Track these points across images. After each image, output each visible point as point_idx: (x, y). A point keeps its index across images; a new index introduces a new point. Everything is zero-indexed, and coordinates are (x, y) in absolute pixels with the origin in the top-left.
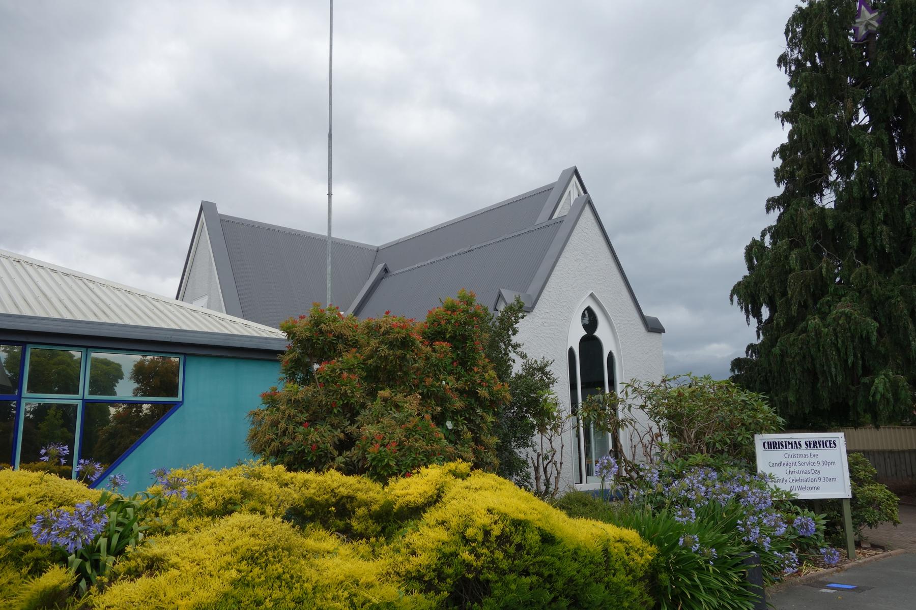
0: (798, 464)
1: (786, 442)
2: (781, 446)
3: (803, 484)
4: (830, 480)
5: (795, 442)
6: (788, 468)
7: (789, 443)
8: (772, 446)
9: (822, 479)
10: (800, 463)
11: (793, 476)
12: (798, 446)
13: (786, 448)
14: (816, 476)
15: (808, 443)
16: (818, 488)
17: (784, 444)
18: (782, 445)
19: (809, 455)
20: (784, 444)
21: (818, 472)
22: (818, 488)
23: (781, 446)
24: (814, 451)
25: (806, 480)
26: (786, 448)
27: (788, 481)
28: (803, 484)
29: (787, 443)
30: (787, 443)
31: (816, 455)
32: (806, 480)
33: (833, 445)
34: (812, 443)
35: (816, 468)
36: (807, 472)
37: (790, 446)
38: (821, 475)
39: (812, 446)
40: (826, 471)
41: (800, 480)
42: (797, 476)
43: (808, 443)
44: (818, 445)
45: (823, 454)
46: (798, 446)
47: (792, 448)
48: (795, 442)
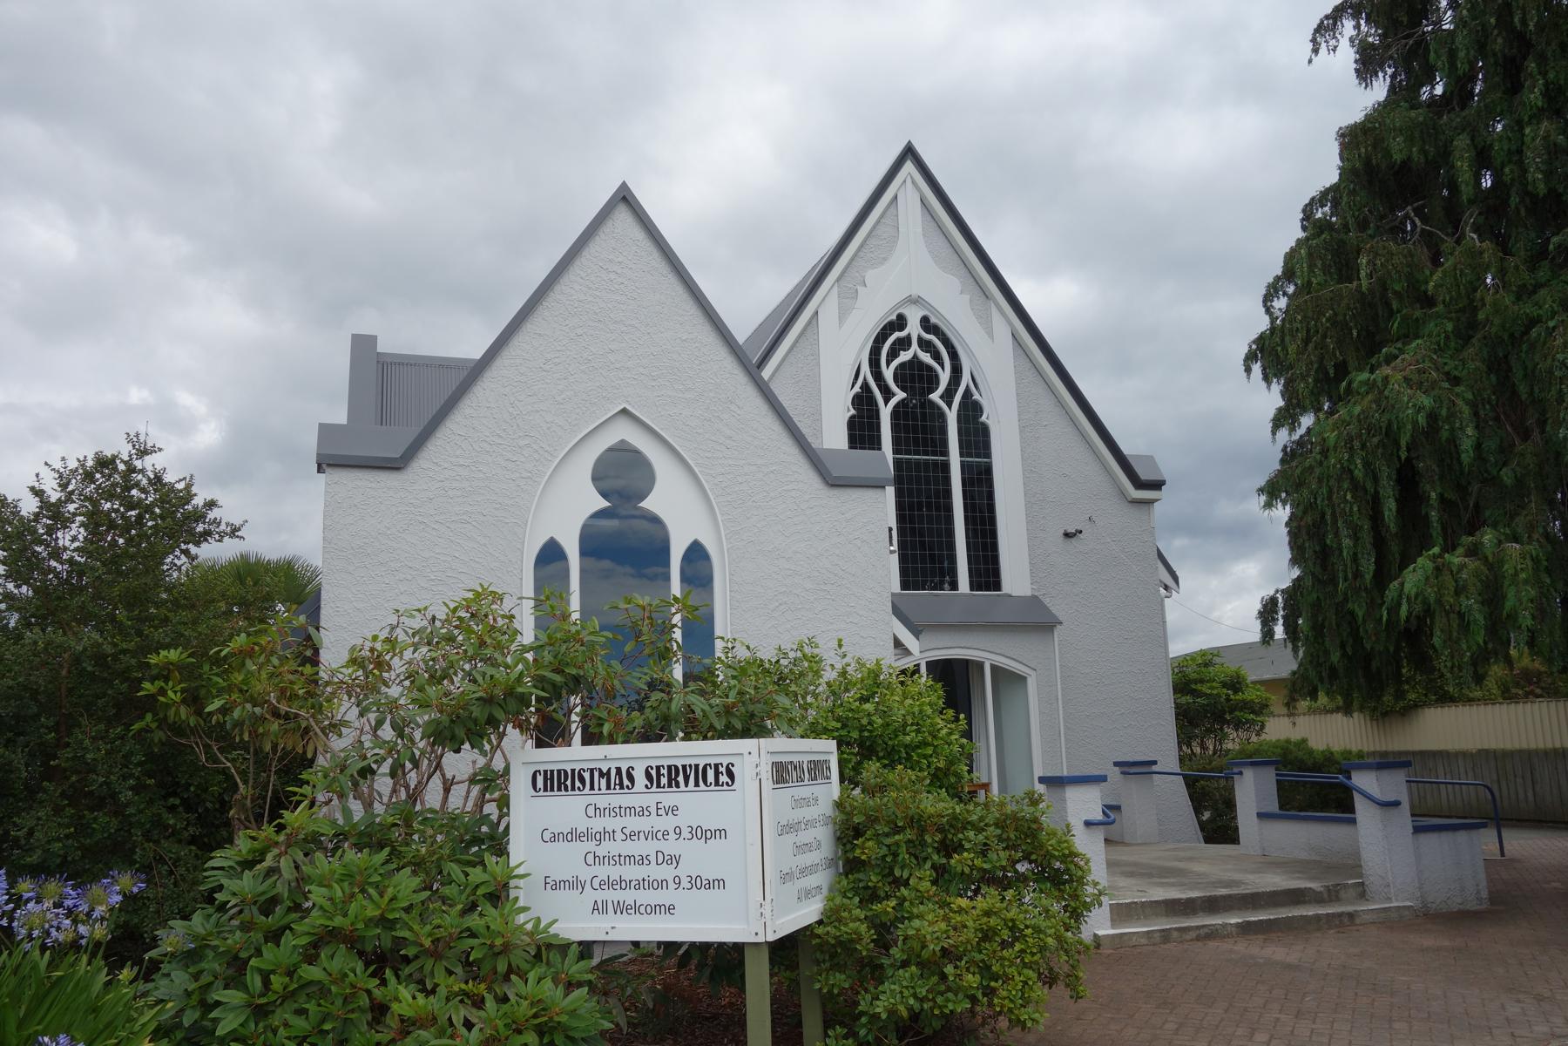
0: (619, 836)
1: (592, 771)
2: (578, 784)
3: (629, 896)
4: (709, 885)
5: (619, 770)
6: (590, 846)
7: (601, 775)
8: (554, 782)
9: (685, 883)
10: (627, 831)
11: (604, 872)
12: (626, 782)
13: (592, 788)
14: (666, 872)
15: (653, 773)
16: (670, 909)
17: (587, 776)
18: (582, 780)
19: (653, 810)
20: (587, 776)
21: (674, 860)
22: (670, 909)
23: (578, 784)
24: (669, 798)
25: (640, 884)
26: (592, 788)
27: (588, 885)
28: (629, 896)
29: (596, 774)
30: (596, 774)
31: (673, 810)
32: (640, 884)
33: (724, 778)
34: (664, 772)
35: (671, 847)
36: (642, 860)
37: (604, 782)
38: (684, 871)
39: (664, 781)
40: (698, 858)
41: (623, 884)
42: (614, 872)
43: (653, 773)
44: (681, 779)
45: (694, 804)
46: (626, 782)
47: (608, 787)
48: (619, 770)
